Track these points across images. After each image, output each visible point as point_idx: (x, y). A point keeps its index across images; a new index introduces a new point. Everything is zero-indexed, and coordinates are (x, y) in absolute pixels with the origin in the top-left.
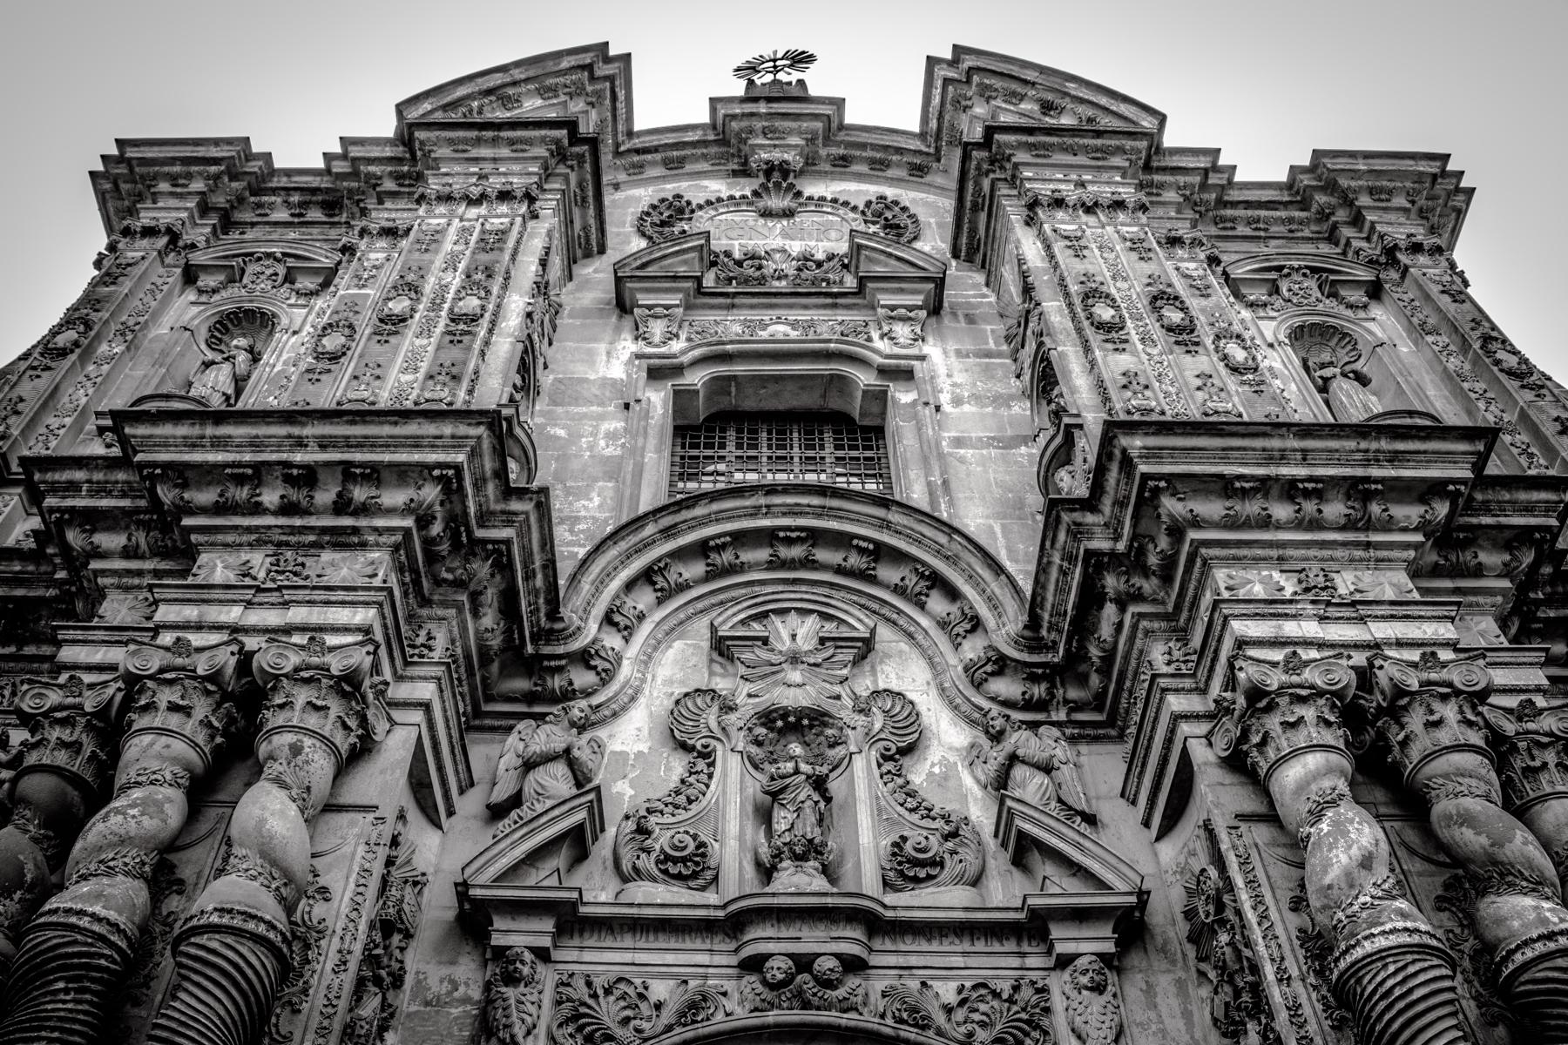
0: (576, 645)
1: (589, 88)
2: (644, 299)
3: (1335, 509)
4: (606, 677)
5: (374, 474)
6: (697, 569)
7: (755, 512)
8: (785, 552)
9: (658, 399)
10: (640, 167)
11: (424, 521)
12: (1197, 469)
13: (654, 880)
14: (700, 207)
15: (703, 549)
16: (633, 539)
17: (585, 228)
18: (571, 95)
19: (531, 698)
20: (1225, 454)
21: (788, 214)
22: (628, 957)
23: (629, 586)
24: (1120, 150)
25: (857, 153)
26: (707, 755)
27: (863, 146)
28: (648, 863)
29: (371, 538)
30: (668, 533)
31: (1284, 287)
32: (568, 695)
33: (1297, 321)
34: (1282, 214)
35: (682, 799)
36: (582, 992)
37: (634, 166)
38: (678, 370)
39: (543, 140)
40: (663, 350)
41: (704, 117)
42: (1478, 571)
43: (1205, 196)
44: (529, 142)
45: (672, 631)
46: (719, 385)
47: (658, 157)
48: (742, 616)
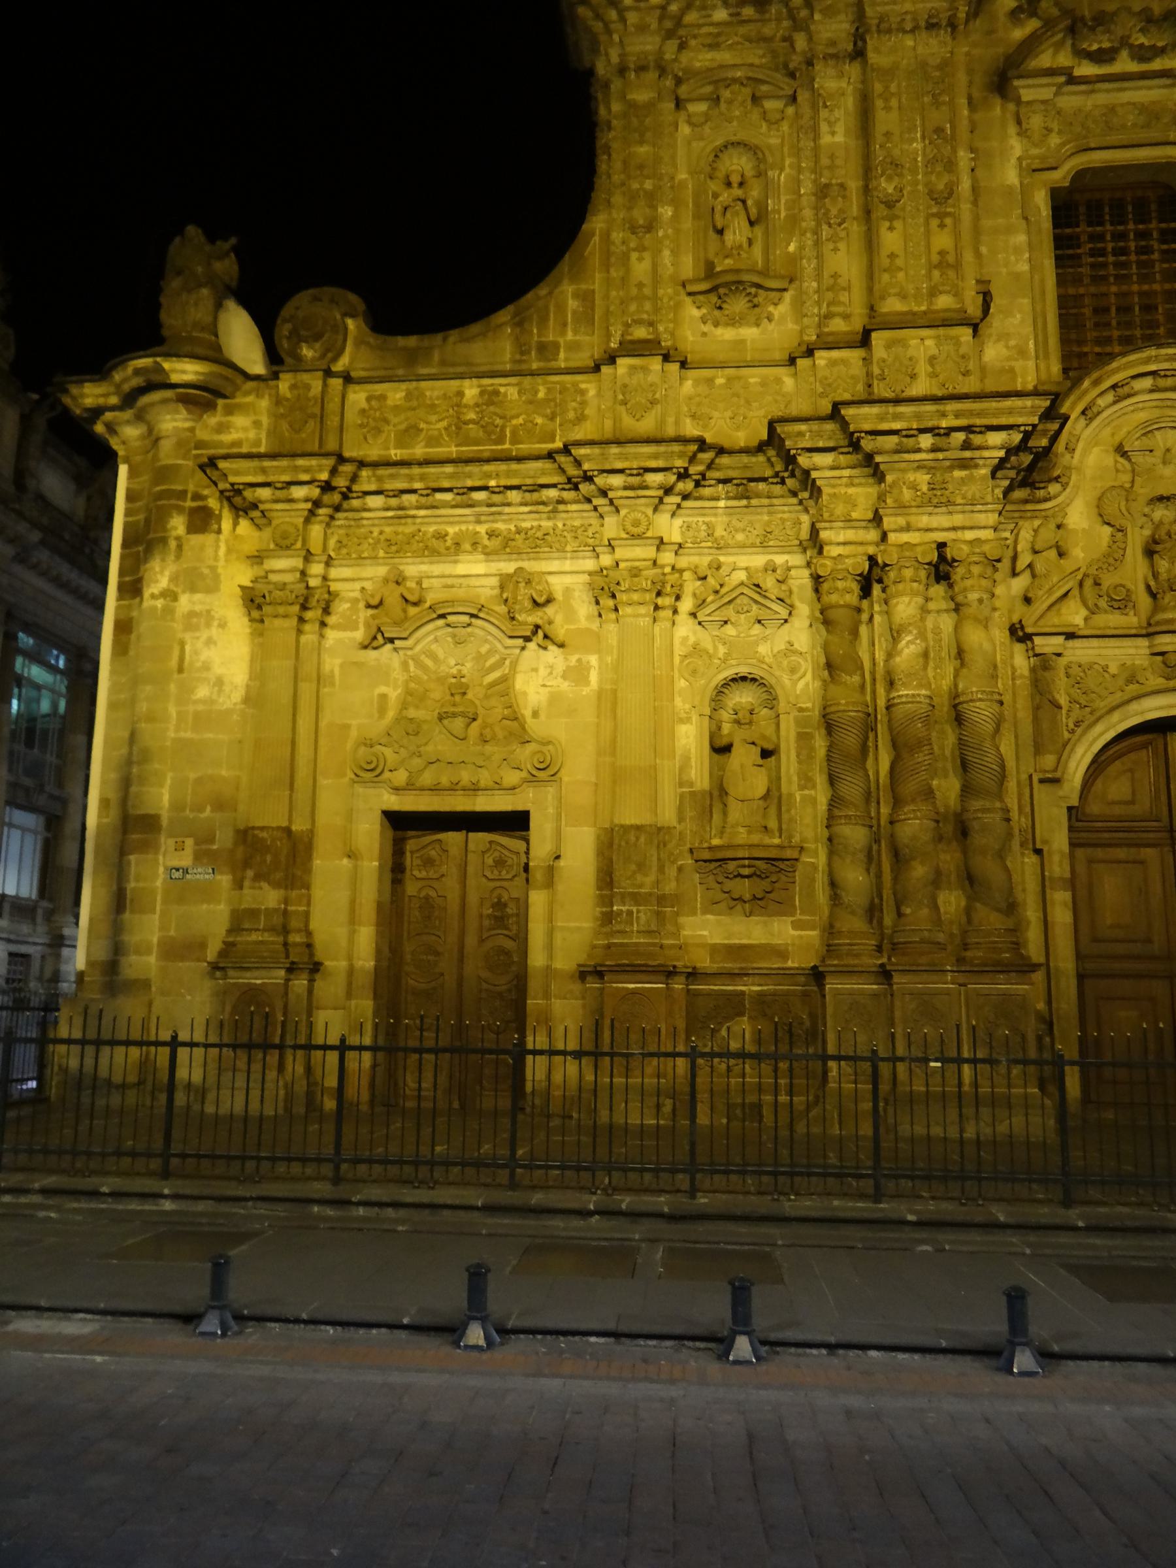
0: (1056, 474)
2: (1026, 95)
4: (1065, 486)
6: (1110, 397)
8: (1162, 383)
13: (1106, 612)
15: (1114, 387)
19: (1026, 501)
22: (1097, 652)
28: (1103, 603)
29: (981, 462)
30: (1096, 383)
32: (1046, 500)
35: (1111, 560)
45: (1094, 442)
46: (1080, 175)
48: (1138, 435)
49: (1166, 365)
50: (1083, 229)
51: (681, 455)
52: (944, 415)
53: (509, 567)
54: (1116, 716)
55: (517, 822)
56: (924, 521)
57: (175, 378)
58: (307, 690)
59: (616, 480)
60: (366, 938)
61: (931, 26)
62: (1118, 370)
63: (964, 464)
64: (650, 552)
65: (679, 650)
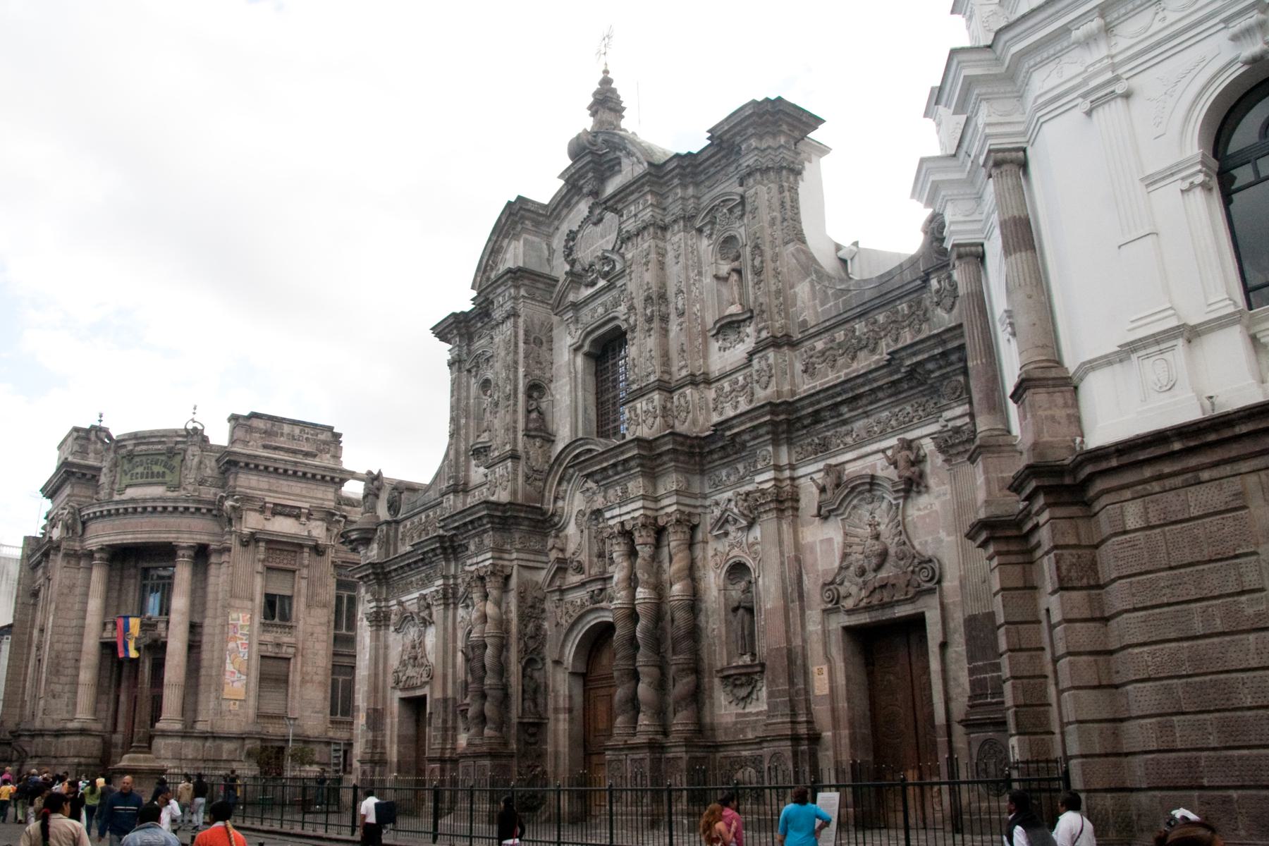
1: (517, 219)
3: (620, 468)
4: (561, 517)
5: (480, 518)
7: (574, 449)
9: (580, 360)
10: (559, 213)
11: (492, 523)
12: (589, 471)
14: (578, 231)
16: (553, 473)
17: (545, 283)
18: (514, 229)
20: (592, 465)
21: (600, 220)
23: (559, 483)
24: (643, 185)
25: (612, 163)
26: (582, 532)
27: (611, 160)
30: (560, 465)
31: (719, 215)
32: (556, 524)
33: (721, 239)
34: (719, 156)
36: (568, 605)
37: (557, 216)
38: (581, 346)
39: (508, 279)
40: (575, 340)
41: (562, 182)
42: (664, 463)
43: (689, 170)
44: (506, 281)
46: (594, 342)
47: (560, 207)
49: (581, 449)
50: (611, 362)
51: (436, 542)
52: (465, 517)
53: (416, 595)
54: (580, 627)
55: (424, 698)
56: (475, 560)
57: (353, 537)
58: (381, 652)
59: (430, 555)
60: (395, 747)
61: (508, 317)
62: (565, 459)
63: (485, 531)
64: (440, 582)
65: (459, 619)
